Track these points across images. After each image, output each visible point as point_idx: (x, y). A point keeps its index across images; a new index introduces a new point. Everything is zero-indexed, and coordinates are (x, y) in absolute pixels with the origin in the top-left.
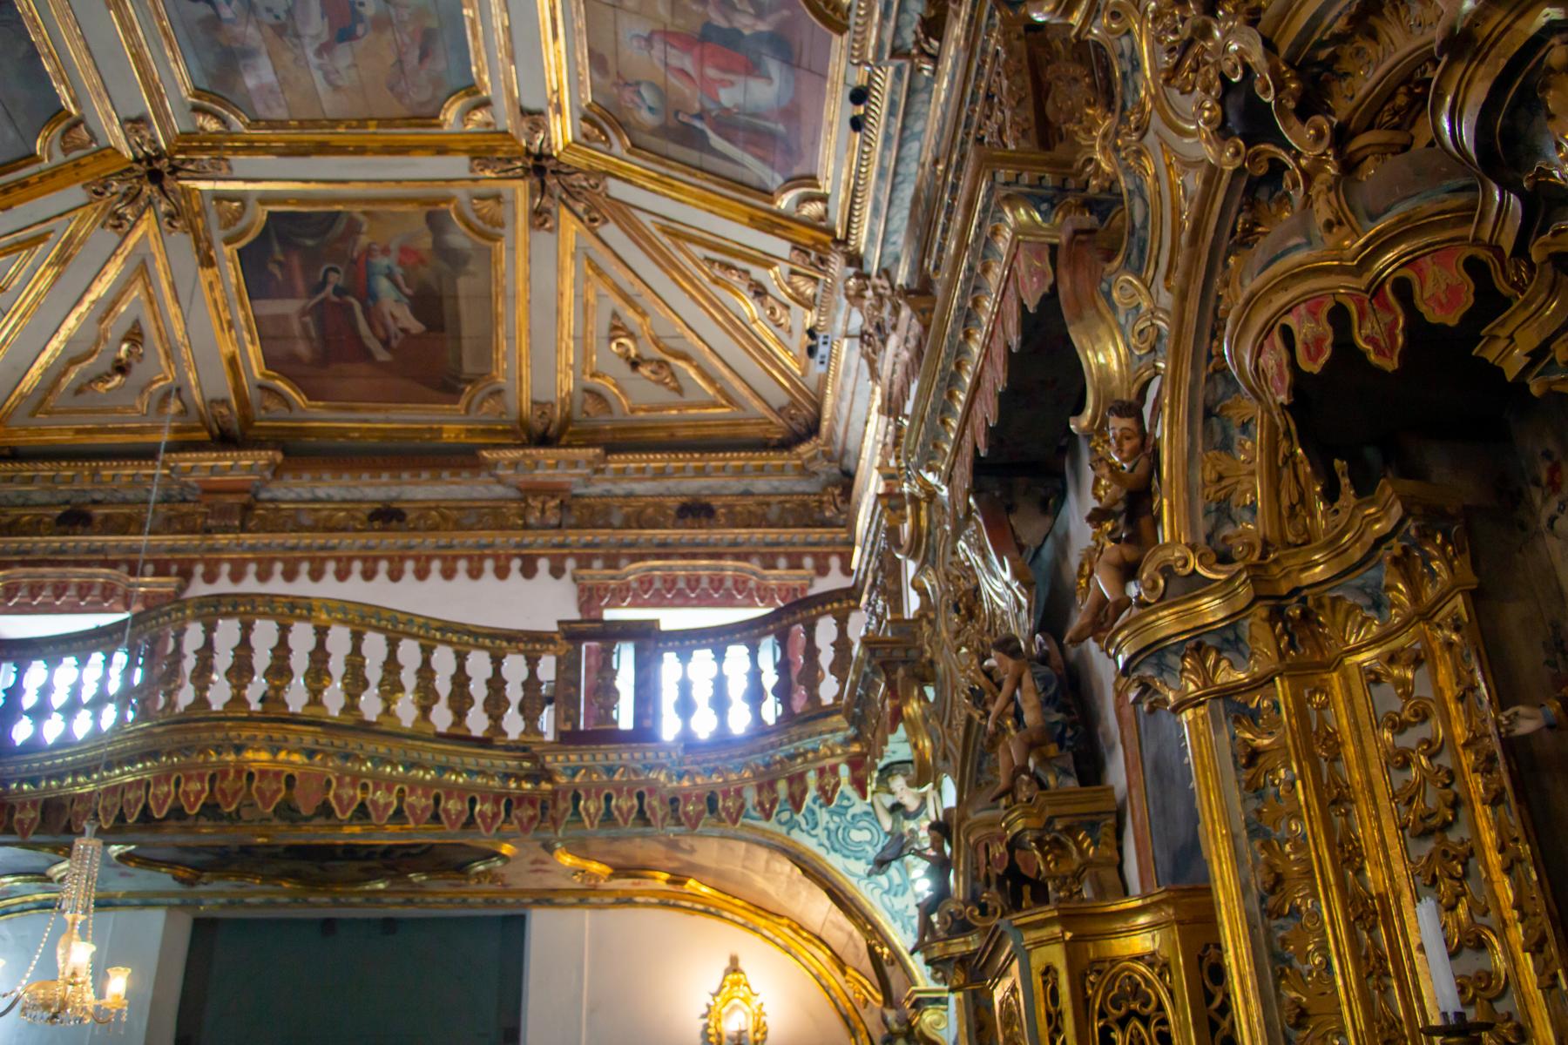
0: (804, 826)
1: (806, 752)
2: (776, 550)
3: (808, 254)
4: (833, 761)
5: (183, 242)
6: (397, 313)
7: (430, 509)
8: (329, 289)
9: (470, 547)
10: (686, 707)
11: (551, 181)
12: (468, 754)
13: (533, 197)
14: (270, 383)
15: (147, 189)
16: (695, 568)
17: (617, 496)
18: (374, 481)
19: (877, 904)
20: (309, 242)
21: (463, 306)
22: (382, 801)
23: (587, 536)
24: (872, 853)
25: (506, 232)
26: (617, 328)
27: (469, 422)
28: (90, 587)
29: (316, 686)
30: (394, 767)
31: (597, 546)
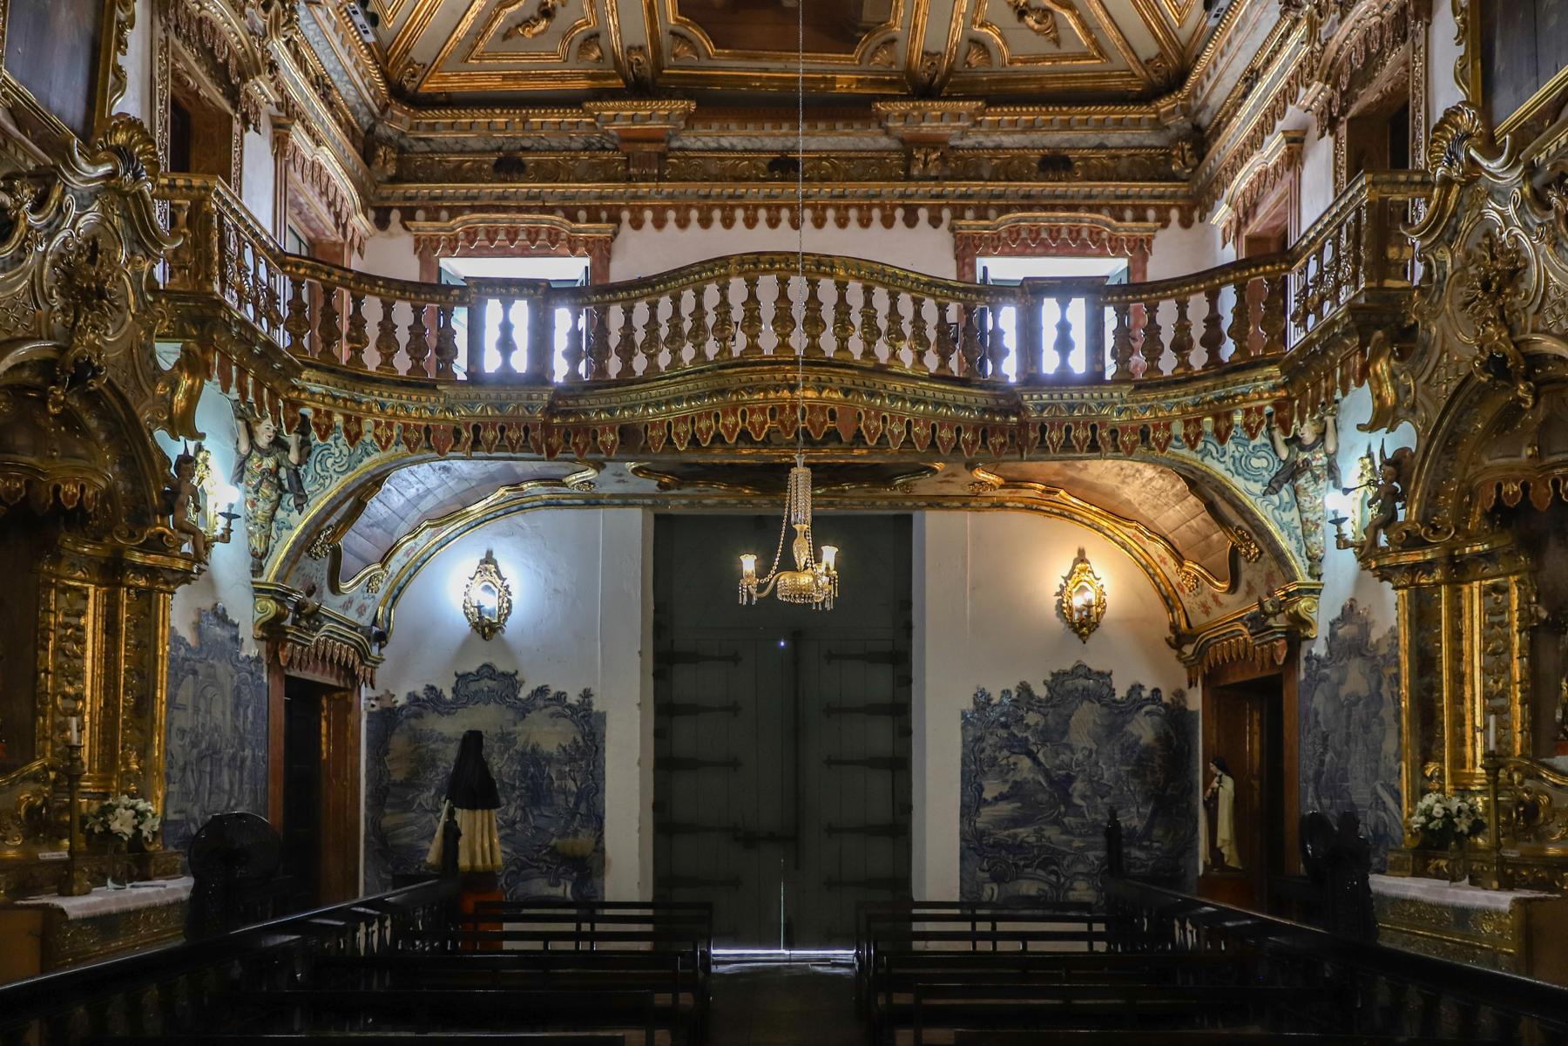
0: (1215, 454)
1: (1236, 395)
2: (1125, 202)
4: (1261, 403)
7: (821, 159)
9: (860, 197)
10: (1064, 345)
16: (1057, 219)
17: (987, 149)
19: (1270, 517)
22: (896, 431)
23: (962, 187)
24: (1267, 477)
29: (842, 335)
30: (883, 398)
31: (970, 197)
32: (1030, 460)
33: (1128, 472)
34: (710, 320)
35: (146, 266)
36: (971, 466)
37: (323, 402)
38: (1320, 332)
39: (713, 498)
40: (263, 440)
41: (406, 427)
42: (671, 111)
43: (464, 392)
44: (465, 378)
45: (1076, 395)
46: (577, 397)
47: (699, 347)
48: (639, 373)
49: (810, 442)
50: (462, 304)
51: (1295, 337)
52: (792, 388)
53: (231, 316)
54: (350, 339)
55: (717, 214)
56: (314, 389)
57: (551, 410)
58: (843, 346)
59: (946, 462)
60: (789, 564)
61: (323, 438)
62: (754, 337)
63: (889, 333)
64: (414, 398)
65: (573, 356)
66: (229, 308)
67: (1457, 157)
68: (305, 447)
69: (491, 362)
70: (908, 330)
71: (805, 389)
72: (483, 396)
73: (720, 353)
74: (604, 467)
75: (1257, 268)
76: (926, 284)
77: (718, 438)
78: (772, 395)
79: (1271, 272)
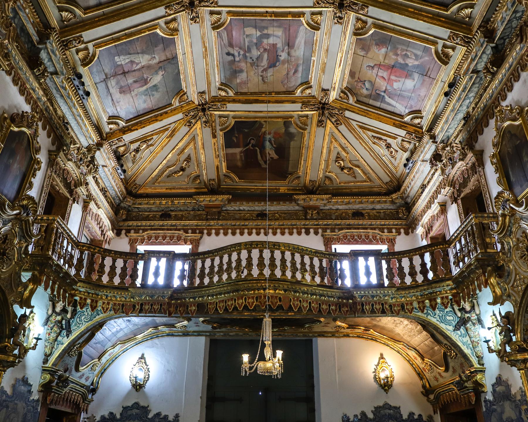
3: (412, 135)
5: (208, 131)
6: (270, 153)
8: (250, 145)
11: (326, 112)
12: (329, 291)
13: (319, 116)
14: (228, 174)
15: (200, 114)
18: (259, 205)
20: (246, 131)
21: (291, 151)
25: (308, 128)
26: (338, 158)
27: (288, 187)
28: (173, 237)
30: (300, 293)
32: (358, 317)
33: (397, 322)
34: (234, 265)
35: (25, 245)
36: (335, 320)
37: (84, 295)
38: (466, 268)
39: (234, 332)
40: (58, 309)
41: (115, 304)
42: (223, 198)
43: (138, 291)
44: (140, 286)
45: (374, 292)
46: (181, 293)
47: (229, 275)
48: (206, 284)
49: (271, 310)
50: (141, 259)
51: (455, 271)
52: (264, 289)
53: (53, 263)
54: (98, 272)
55: (238, 231)
56: (81, 290)
57: (171, 298)
58: (284, 273)
59: (325, 318)
60: (262, 358)
61: (81, 308)
62: (250, 270)
63: (301, 269)
64: (119, 293)
65: (182, 277)
66: (53, 260)
67: (506, 207)
68: (74, 313)
69: (151, 281)
70: (308, 268)
71: (269, 290)
72: (146, 292)
73: (237, 276)
74: (191, 320)
75: (437, 246)
76: (314, 252)
77: (235, 308)
78: (256, 292)
79: (443, 248)
